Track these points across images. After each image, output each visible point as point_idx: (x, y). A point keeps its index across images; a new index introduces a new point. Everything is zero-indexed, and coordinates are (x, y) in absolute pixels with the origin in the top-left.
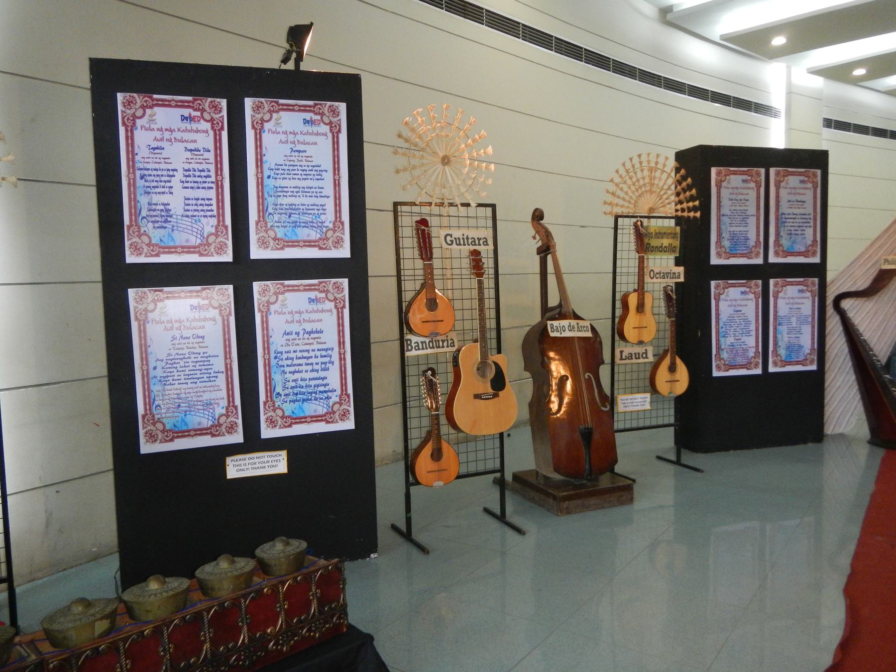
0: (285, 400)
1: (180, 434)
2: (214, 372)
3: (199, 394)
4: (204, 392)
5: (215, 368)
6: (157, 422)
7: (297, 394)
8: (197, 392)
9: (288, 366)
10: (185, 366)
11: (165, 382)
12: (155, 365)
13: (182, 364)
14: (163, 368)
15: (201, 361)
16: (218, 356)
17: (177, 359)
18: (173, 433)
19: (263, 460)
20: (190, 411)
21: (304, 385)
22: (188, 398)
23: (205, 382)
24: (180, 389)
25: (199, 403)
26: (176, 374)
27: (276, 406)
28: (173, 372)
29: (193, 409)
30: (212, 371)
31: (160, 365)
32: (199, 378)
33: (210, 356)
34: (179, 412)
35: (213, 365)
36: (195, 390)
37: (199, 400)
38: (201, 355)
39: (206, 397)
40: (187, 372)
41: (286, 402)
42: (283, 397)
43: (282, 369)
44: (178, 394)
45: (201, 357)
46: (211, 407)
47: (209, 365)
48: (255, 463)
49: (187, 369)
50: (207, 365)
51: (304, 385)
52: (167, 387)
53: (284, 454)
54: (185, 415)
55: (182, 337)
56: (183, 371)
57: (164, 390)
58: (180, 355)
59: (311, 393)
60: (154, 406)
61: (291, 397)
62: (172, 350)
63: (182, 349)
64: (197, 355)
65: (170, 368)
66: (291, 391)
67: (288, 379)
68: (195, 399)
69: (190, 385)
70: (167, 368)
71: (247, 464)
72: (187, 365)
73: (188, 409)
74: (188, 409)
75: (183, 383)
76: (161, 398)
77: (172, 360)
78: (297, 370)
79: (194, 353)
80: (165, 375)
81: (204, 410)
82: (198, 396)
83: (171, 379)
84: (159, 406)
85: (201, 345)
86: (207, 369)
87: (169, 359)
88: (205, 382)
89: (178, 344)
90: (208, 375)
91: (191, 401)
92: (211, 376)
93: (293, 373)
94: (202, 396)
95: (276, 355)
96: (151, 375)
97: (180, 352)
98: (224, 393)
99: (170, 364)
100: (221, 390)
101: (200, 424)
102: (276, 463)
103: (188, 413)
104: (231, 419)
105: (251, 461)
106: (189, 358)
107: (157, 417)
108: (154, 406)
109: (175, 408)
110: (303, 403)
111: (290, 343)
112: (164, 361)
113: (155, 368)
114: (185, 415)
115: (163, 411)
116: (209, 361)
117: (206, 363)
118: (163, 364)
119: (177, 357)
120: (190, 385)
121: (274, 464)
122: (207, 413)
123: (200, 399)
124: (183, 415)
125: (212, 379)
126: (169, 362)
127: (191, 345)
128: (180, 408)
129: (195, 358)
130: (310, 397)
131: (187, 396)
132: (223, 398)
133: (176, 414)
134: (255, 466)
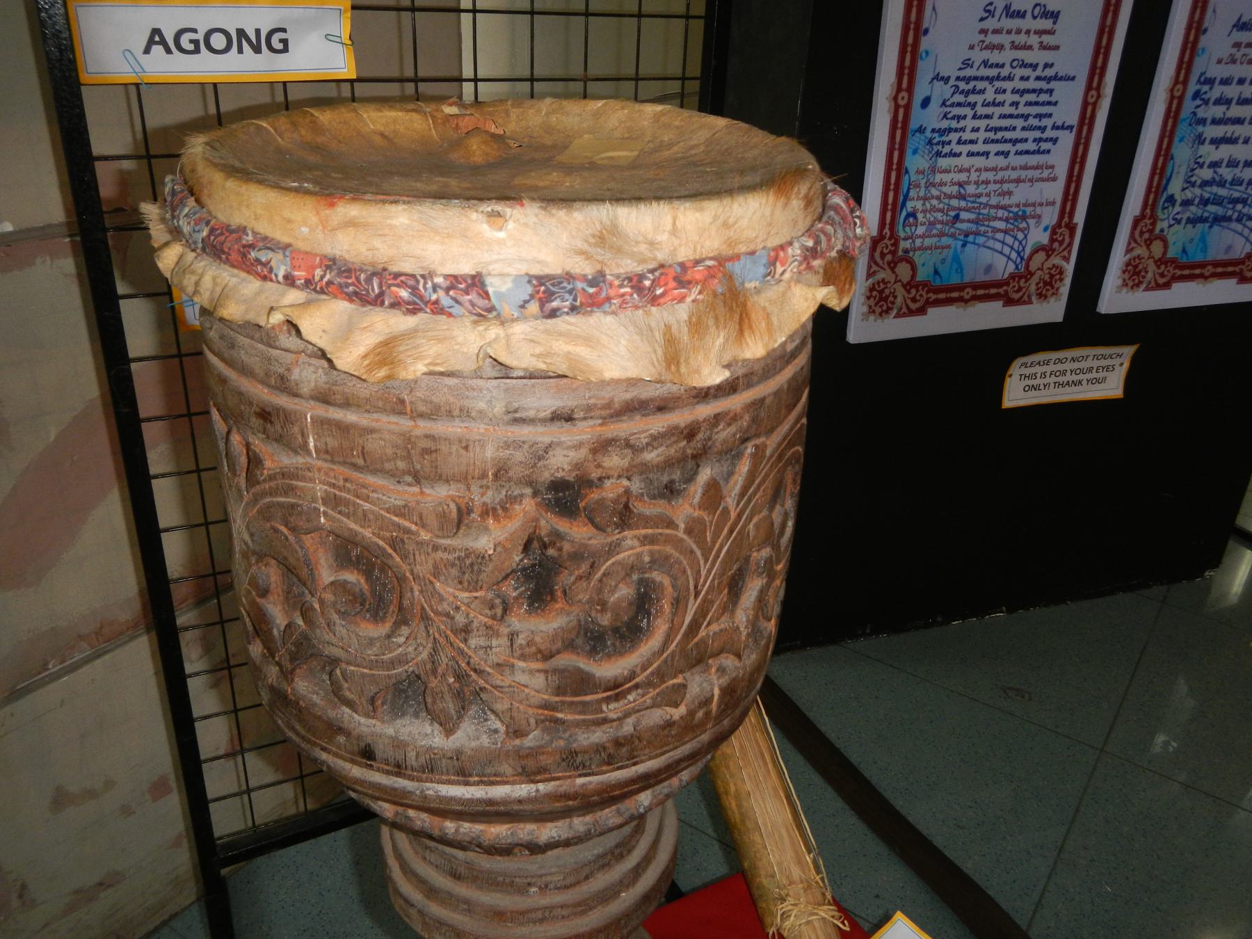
0: (1178, 217)
1: (942, 296)
2: (1055, 127)
3: (1006, 187)
4: (1018, 181)
5: (1058, 118)
6: (901, 260)
7: (1205, 202)
8: (1002, 182)
9: (1215, 122)
10: (994, 104)
11: (940, 147)
12: (928, 93)
13: (990, 95)
14: (944, 104)
15: (1034, 91)
16: (1073, 79)
17: (982, 79)
18: (928, 292)
19: (1083, 365)
20: (977, 234)
21: (1229, 178)
22: (979, 196)
23: (1027, 152)
24: (968, 170)
25: (1000, 213)
26: (969, 123)
27: (1157, 231)
28: (965, 117)
29: (982, 229)
30: (1047, 122)
31: (941, 91)
32: (1015, 142)
33: (1055, 78)
34: (953, 236)
35: (1056, 104)
36: (1000, 175)
37: (1003, 203)
38: (1039, 72)
39: (1021, 194)
40: (995, 122)
41: (1179, 222)
42: (1178, 208)
43: (1200, 128)
44: (960, 185)
45: (1038, 78)
46: (1024, 225)
47: (1049, 103)
48: (1064, 373)
49: (998, 111)
50: (1043, 104)
51: (1229, 178)
52: (943, 163)
53: (1128, 351)
54: (964, 245)
55: (1007, 8)
56: (987, 117)
57: (933, 170)
58: (991, 66)
59: (1235, 201)
60: (904, 213)
61: (1193, 208)
62: (977, 49)
63: (1000, 47)
64: (1027, 72)
65: (959, 104)
66: (1197, 191)
67: (1201, 160)
68: (994, 201)
69: (994, 161)
70: (952, 105)
71: (1048, 374)
72: (1000, 98)
73: (973, 227)
74: (973, 227)
75: (978, 154)
76: (922, 194)
77: (968, 80)
78: (1229, 135)
79: (1024, 65)
80: (945, 124)
81: (1006, 232)
82: (1003, 194)
83: (954, 137)
84: (913, 215)
85: (1046, 39)
86: (1040, 116)
87: (964, 79)
88: (1027, 152)
89: (996, 32)
90: (1037, 134)
91: (986, 205)
92: (1044, 136)
93: (1216, 142)
94: (1010, 193)
95: (1199, 87)
96: (913, 125)
97: (995, 57)
98: (1055, 191)
99: (962, 92)
100: (1054, 179)
101: (989, 269)
102: (1105, 374)
103: (971, 238)
104: (1056, 260)
105: (1060, 367)
106: (1010, 78)
107: (904, 245)
108: (904, 213)
109: (947, 224)
110: (1211, 227)
111: (1238, 55)
112: (952, 82)
113: (926, 103)
114: (964, 245)
115: (921, 230)
116: (1051, 91)
117: (1044, 97)
118: (947, 90)
119: (985, 72)
120: (994, 161)
121: (1101, 375)
122: (1009, 240)
123: (1006, 201)
124: (960, 243)
125: (1044, 146)
126: (962, 85)
127: (1021, 39)
128: (958, 225)
129: (1022, 78)
130: (1230, 213)
131: (981, 189)
132: (1053, 203)
133: (945, 241)
134: (1061, 379)
